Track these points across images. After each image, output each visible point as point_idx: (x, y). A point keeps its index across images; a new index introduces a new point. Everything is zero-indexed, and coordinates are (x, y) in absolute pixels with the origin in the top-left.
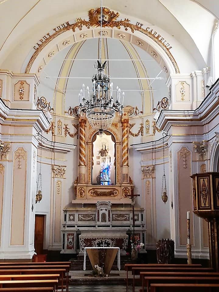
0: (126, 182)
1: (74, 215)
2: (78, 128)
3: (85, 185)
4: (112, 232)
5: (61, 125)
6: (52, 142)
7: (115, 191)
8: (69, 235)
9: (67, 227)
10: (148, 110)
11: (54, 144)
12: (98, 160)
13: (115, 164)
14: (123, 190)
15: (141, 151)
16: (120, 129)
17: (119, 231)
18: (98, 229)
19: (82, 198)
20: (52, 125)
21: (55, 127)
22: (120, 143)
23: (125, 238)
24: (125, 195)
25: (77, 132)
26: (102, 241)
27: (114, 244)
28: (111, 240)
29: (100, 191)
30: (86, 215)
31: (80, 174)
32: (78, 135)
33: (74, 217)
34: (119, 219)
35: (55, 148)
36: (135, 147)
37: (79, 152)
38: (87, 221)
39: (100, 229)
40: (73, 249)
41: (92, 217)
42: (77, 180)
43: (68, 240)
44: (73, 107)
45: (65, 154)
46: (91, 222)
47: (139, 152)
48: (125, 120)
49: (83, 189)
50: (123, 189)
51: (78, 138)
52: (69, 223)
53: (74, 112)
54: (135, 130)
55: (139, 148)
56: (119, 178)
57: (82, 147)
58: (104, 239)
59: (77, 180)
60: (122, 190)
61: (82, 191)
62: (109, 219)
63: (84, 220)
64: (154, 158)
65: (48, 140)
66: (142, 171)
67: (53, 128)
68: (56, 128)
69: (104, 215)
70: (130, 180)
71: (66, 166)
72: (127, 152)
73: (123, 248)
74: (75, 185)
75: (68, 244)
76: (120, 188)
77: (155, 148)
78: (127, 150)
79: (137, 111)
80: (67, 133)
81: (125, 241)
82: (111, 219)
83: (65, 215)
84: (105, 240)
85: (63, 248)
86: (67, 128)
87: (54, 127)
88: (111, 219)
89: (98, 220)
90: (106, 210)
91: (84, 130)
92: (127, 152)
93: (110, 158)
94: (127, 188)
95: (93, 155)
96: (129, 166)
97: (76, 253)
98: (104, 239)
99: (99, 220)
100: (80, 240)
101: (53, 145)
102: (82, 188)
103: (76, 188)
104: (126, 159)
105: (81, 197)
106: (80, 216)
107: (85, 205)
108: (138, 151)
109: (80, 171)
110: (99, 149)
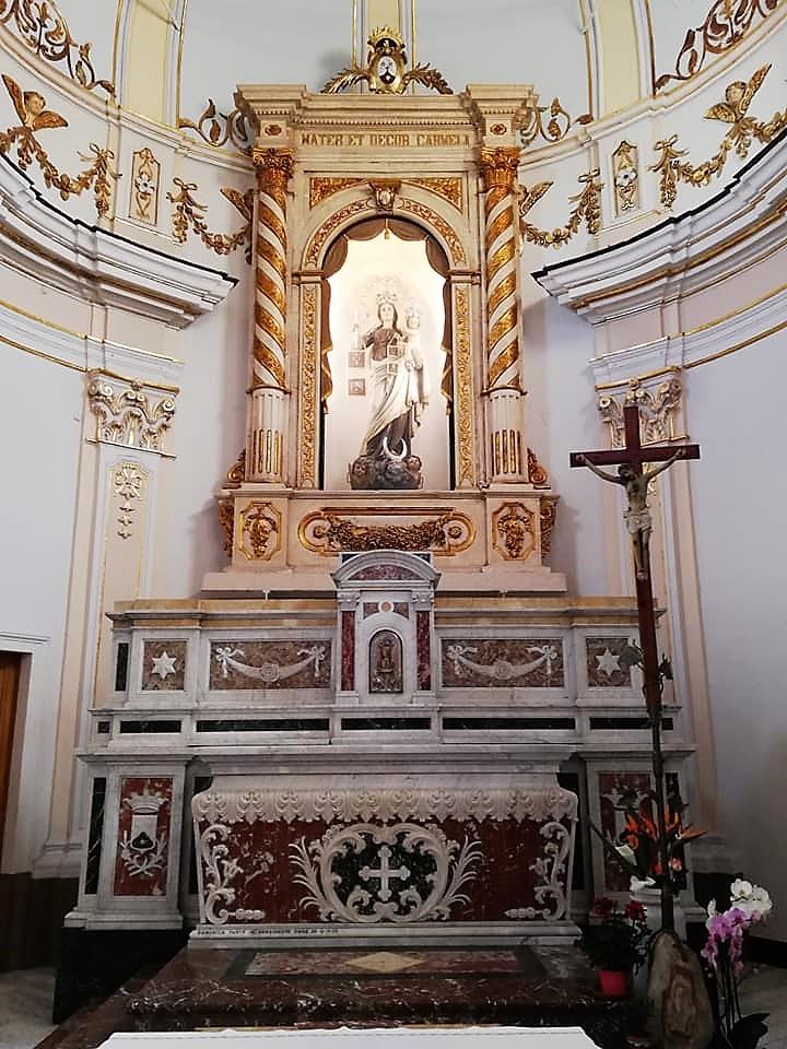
0: (510, 476)
1: (178, 650)
2: (251, 208)
3: (280, 488)
4: (442, 769)
5: (155, 177)
6: (77, 222)
7: (452, 524)
8: (134, 786)
9: (127, 727)
10: (622, 87)
11: (94, 241)
12: (359, 373)
13: (448, 385)
14: (498, 519)
15: (592, 305)
16: (474, 205)
17: (508, 760)
18: (338, 748)
19: (260, 562)
20: (101, 163)
21: (117, 177)
22: (474, 275)
23: (551, 819)
24: (509, 546)
25: (247, 232)
26: (368, 838)
27: (464, 861)
28: (440, 826)
29: (368, 525)
30: (267, 645)
31: (256, 436)
32: (251, 244)
33: (181, 661)
34: (492, 671)
35: (103, 268)
36: (560, 280)
37: (252, 320)
38: (273, 686)
39: (358, 748)
40: (156, 890)
41: (306, 662)
42: (239, 469)
43: (125, 824)
44: (227, 106)
45: (171, 333)
46: (297, 691)
47: (580, 312)
48: (498, 151)
49: (267, 512)
50: (496, 513)
51: (249, 260)
52: (141, 700)
53: (230, 132)
54: (550, 214)
55: (578, 282)
56: (472, 453)
57: (271, 295)
58: (391, 823)
59: (241, 471)
60: (489, 518)
61: (263, 523)
62: (421, 669)
63: (254, 684)
64: (673, 330)
65: (38, 199)
66: (600, 409)
67: (102, 179)
68: (124, 185)
69: (385, 645)
70: (534, 469)
71: (176, 391)
72: (514, 322)
73: (538, 897)
74: (227, 492)
75: (126, 855)
76: (479, 506)
77: (688, 265)
78: (514, 310)
79: (561, 121)
80: (191, 225)
81: (554, 840)
82: (436, 672)
83: (124, 651)
84: (398, 827)
85: (92, 888)
86: (195, 205)
87: (109, 178)
88: (436, 672)
89: (348, 682)
90: (401, 610)
91: (281, 211)
92: (514, 322)
93: (420, 371)
94: (521, 505)
95: (326, 341)
96: (523, 394)
97: (180, 927)
98: (391, 823)
99: (352, 679)
100: (202, 831)
101: (83, 239)
102: (261, 506)
103: (230, 511)
104: (508, 352)
105: (258, 554)
106: (225, 654)
107: (275, 595)
108: (574, 306)
109: (254, 420)
110: (371, 325)
